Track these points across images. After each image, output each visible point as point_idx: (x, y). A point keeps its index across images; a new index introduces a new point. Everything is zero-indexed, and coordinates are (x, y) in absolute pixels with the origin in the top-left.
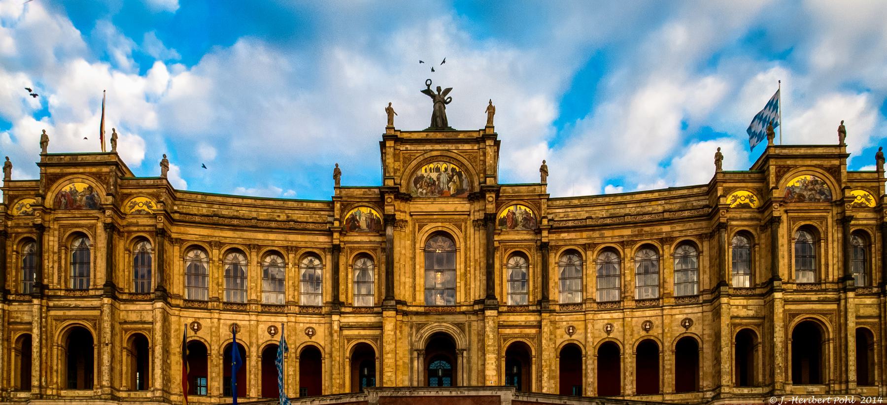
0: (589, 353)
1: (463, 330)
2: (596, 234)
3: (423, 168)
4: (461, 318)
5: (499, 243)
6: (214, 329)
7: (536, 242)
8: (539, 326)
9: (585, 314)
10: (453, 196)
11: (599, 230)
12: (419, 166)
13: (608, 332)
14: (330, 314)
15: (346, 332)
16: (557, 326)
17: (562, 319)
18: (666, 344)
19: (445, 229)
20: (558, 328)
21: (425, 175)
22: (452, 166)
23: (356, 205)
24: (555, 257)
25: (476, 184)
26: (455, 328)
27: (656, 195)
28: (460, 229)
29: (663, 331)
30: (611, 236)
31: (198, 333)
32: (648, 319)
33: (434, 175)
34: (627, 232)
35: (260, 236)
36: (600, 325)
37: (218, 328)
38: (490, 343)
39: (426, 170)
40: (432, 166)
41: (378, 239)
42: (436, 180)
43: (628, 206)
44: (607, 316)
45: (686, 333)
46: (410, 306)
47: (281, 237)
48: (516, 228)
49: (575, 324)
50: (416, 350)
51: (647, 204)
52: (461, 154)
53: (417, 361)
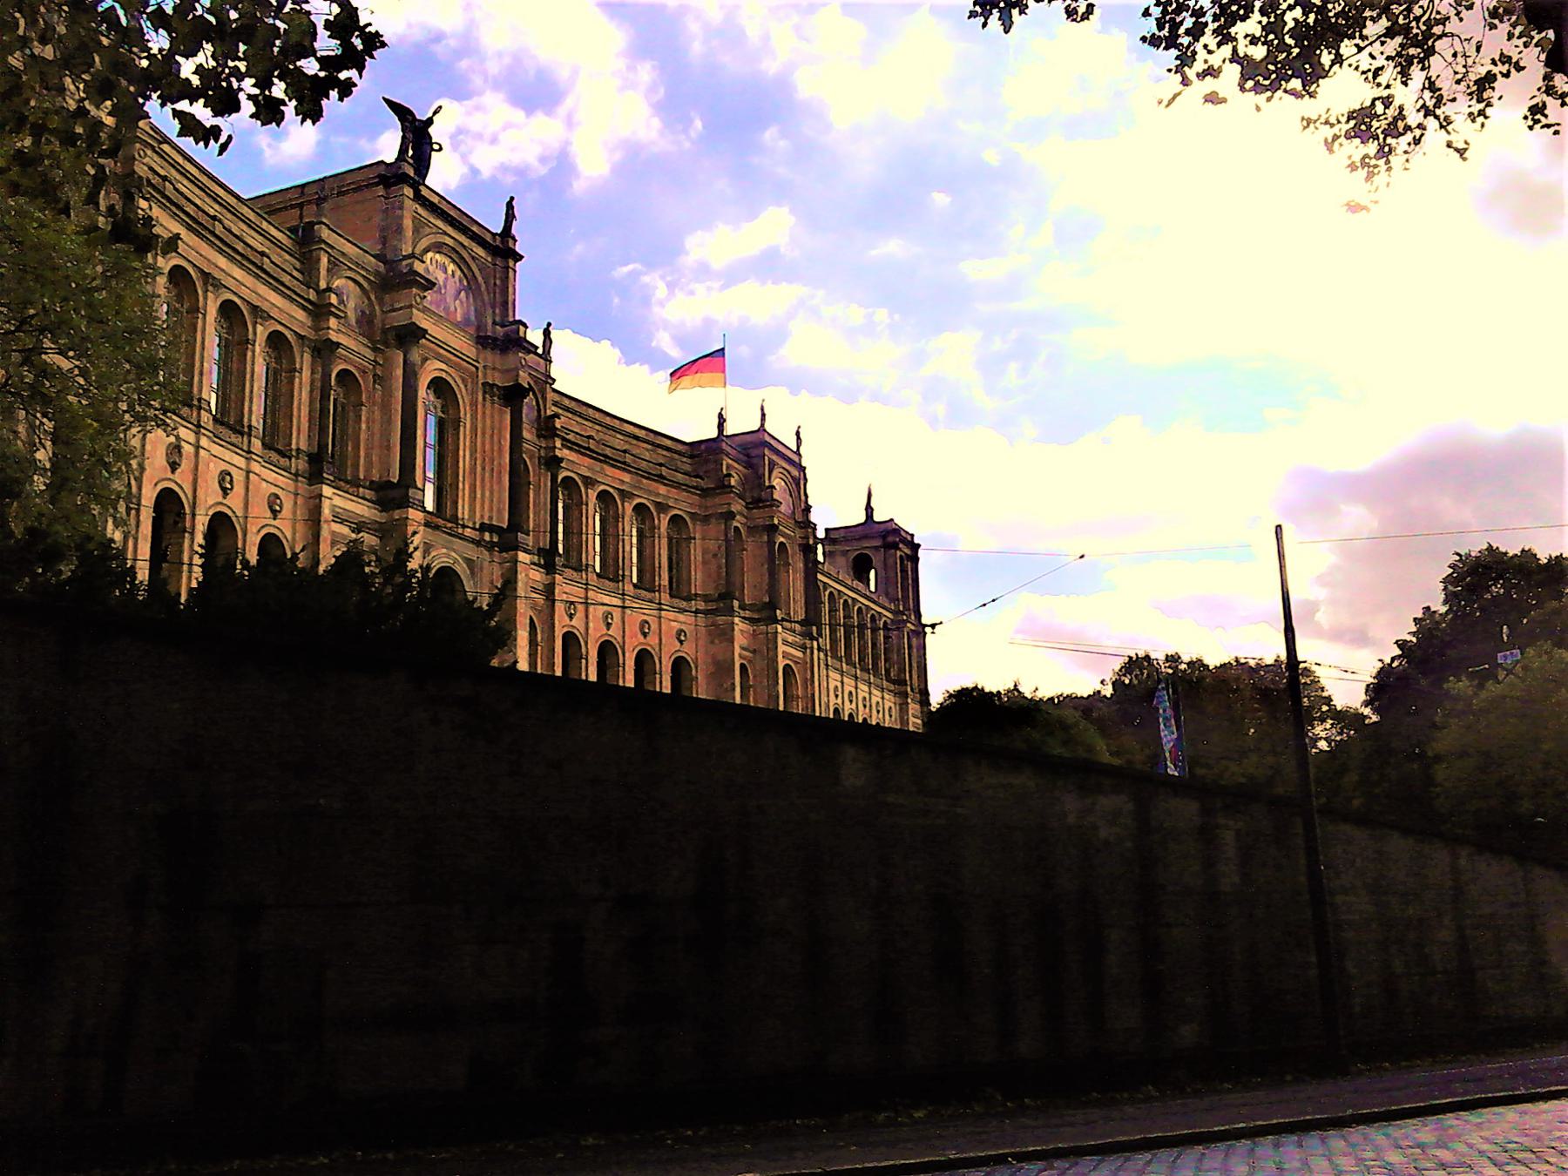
0: (591, 654)
1: (473, 573)
2: (598, 466)
3: (430, 255)
4: (472, 552)
7: (539, 450)
8: (549, 591)
9: (586, 589)
10: (456, 325)
11: (601, 461)
12: (426, 250)
13: (609, 625)
14: (315, 477)
15: (337, 527)
18: (664, 662)
19: (449, 379)
21: (431, 268)
23: (352, 275)
25: (490, 321)
26: (465, 566)
27: (641, 434)
28: (466, 386)
29: (660, 640)
30: (612, 478)
32: (645, 618)
33: (439, 277)
34: (627, 477)
35: (222, 262)
38: (522, 611)
39: (431, 259)
40: (438, 256)
41: (369, 354)
43: (619, 436)
44: (607, 600)
45: (679, 650)
47: (249, 280)
51: (635, 442)
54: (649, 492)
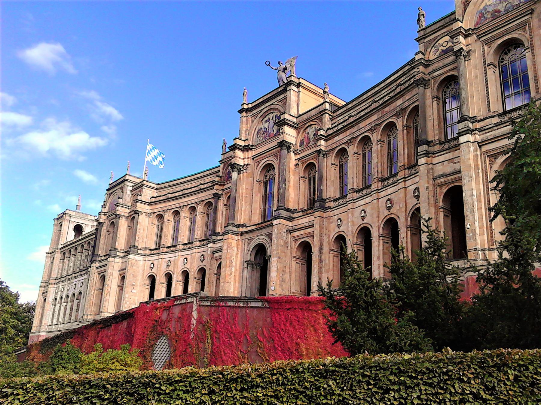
2: (355, 129)
5: (299, 160)
6: (159, 266)
13: (363, 218)
16: (331, 221)
17: (334, 213)
20: (332, 223)
22: (275, 114)
24: (331, 160)
26: (267, 239)
31: (153, 270)
32: (389, 197)
35: (186, 199)
36: (357, 213)
37: (161, 265)
42: (267, 127)
46: (248, 227)
48: (309, 145)
49: (340, 216)
50: (245, 262)
52: (278, 103)
53: (246, 270)
54: (390, 112)
